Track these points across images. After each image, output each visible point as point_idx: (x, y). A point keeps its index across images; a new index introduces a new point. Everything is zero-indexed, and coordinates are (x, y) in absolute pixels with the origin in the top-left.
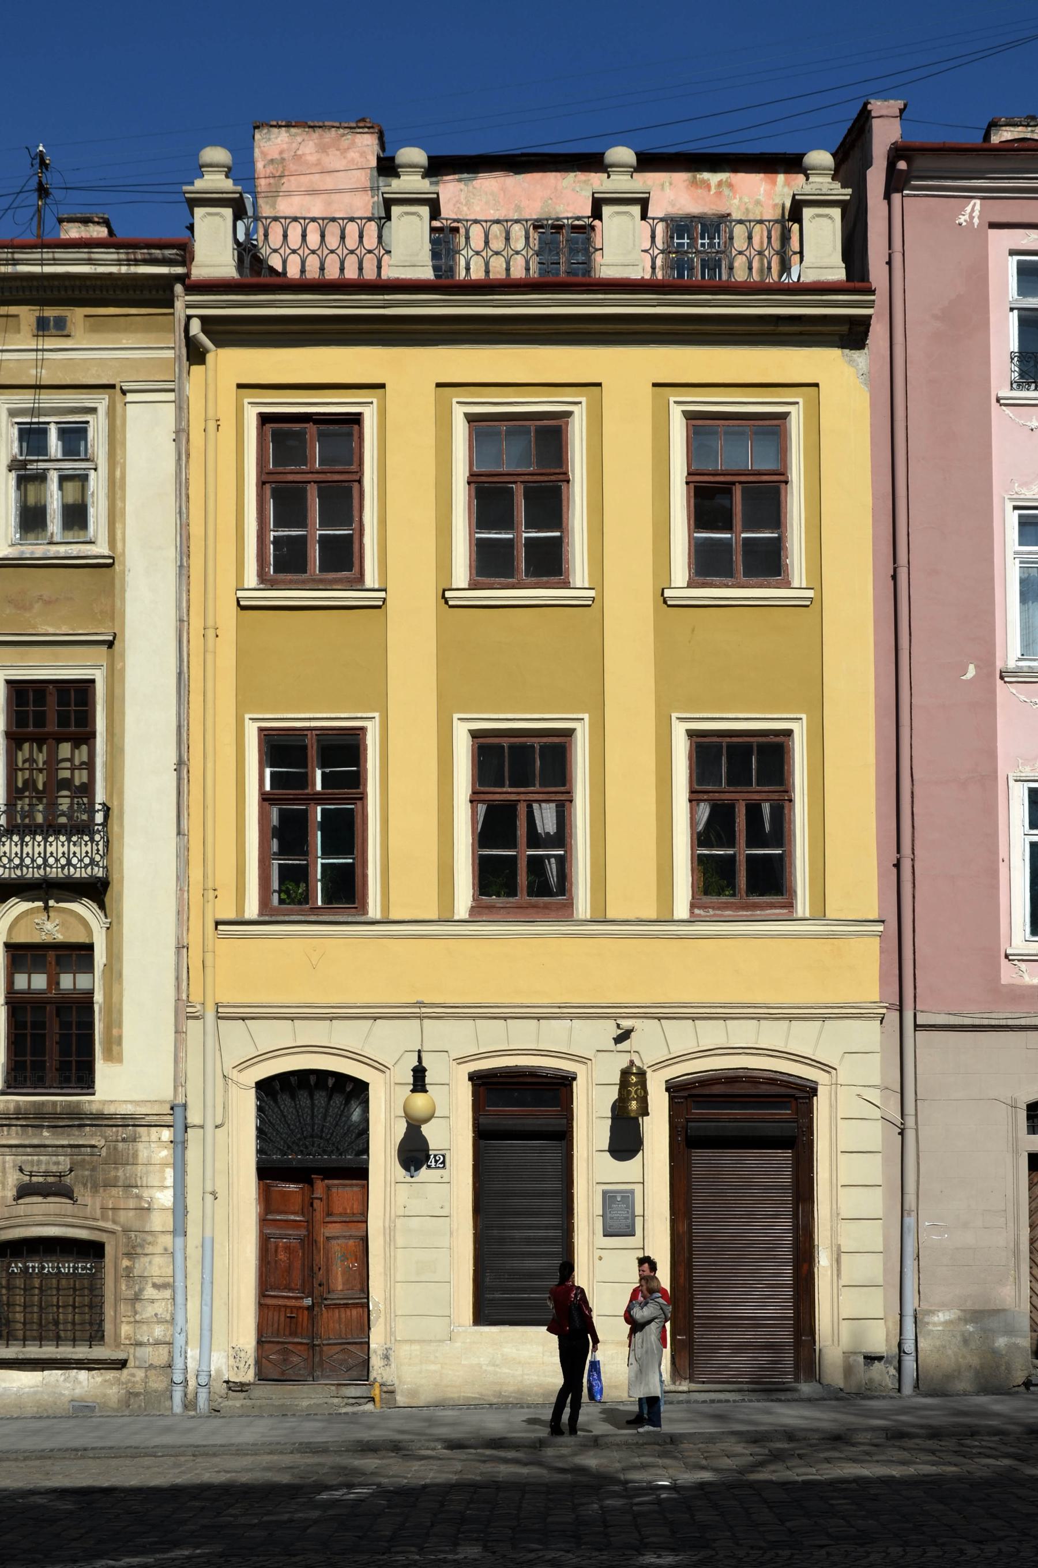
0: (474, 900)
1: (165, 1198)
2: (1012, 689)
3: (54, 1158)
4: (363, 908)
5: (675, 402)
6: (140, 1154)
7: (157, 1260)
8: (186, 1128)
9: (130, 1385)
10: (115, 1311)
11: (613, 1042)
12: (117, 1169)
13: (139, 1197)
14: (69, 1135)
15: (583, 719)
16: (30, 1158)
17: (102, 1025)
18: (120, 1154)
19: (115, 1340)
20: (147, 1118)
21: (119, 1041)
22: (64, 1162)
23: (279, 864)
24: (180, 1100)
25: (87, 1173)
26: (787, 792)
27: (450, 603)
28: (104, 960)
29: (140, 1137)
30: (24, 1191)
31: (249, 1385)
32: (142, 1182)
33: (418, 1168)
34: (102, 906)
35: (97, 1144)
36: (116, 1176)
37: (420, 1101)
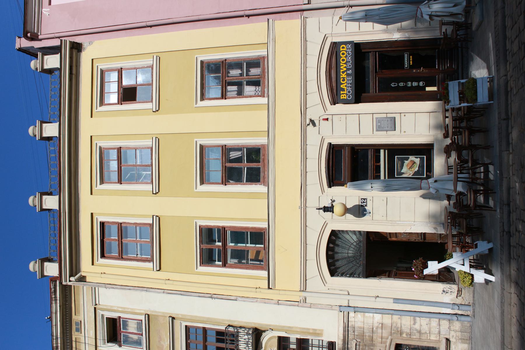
0: (261, 185)
1: (378, 317)
5: (96, 109)
6: (360, 326)
8: (349, 306)
9: (457, 338)
10: (425, 341)
11: (315, 127)
12: (365, 336)
13: (377, 328)
15: (196, 141)
18: (359, 334)
19: (437, 343)
20: (345, 321)
23: (250, 261)
24: (338, 308)
25: (367, 348)
26: (223, 61)
27: (157, 191)
28: (284, 333)
29: (353, 325)
31: (459, 288)
32: (371, 326)
33: (365, 210)
34: (264, 331)
35: (355, 343)
36: (369, 336)
37: (338, 209)
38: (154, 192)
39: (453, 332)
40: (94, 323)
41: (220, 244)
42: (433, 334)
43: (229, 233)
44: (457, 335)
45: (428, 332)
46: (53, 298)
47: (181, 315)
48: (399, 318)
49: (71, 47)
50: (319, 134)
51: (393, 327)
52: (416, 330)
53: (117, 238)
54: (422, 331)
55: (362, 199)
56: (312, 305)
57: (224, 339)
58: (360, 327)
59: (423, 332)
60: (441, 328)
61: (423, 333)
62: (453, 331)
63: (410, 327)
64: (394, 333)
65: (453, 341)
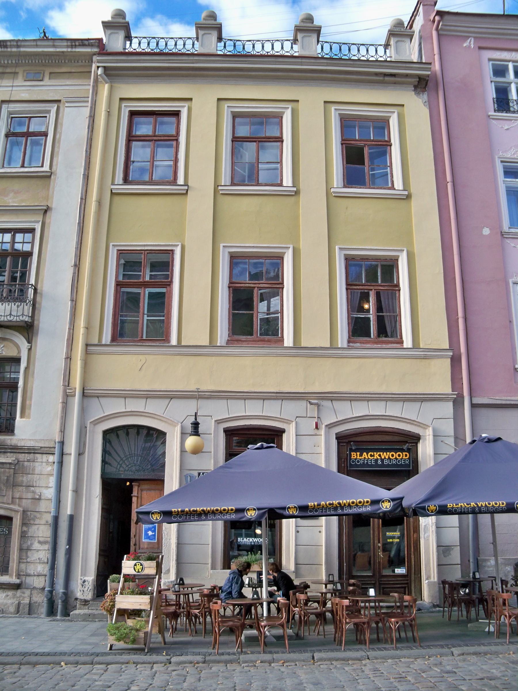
0: (229, 337)
2: (508, 241)
4: (167, 339)
12: (23, 476)
13: (34, 492)
31: (89, 601)
32: (36, 484)
36: (22, 480)
38: (220, 188)
39: (29, 593)
41: (147, 279)
43: (163, 290)
44: (25, 599)
45: (29, 560)
46: (75, 43)
47: (50, 222)
48: (47, 522)
49: (421, 77)
50: (297, 417)
51: (35, 513)
53: (157, 134)
54: (31, 552)
56: (65, 404)
57: (16, 282)
58: (34, 469)
60: (35, 578)
61: (27, 554)
62: (31, 594)
63: (35, 536)
65: (17, 592)
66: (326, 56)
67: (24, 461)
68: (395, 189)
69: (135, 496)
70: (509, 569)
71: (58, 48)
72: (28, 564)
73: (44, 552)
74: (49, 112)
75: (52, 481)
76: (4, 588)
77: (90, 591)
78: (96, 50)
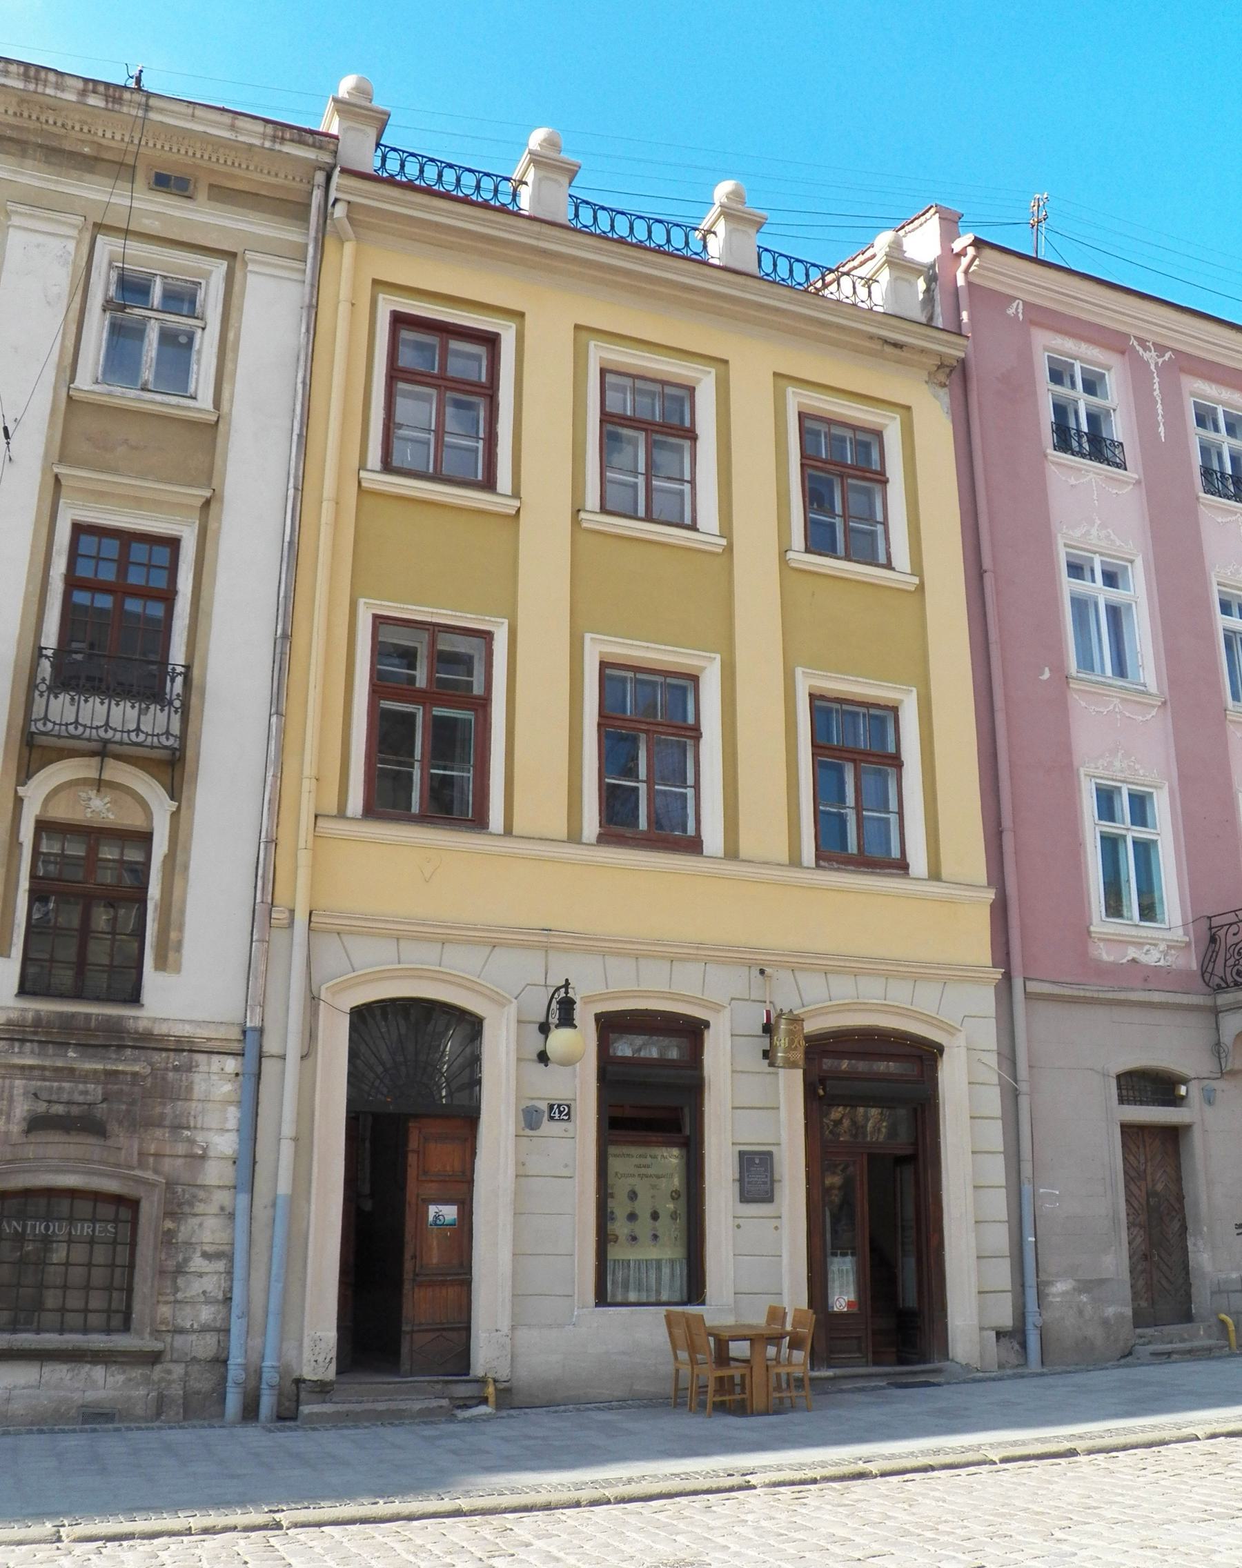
0: (600, 826)
3: (81, 1087)
6: (196, 1088)
7: (211, 1223)
12: (164, 1104)
13: (191, 1141)
14: (103, 1058)
16: (47, 1083)
17: (156, 926)
21: (179, 946)
22: (95, 1091)
24: (256, 1023)
25: (124, 1107)
29: (197, 1066)
30: (36, 1124)
32: (196, 1123)
35: (142, 1071)
36: (163, 1113)
39: (182, 1372)
40: (185, 239)
42: (174, 1311)
44: (173, 1386)
45: (180, 1296)
50: (733, 999)
51: (195, 1190)
52: (187, 1260)
55: (569, 1106)
59: (178, 1281)
60: (194, 1337)
61: (176, 1282)
62: (186, 1374)
63: (194, 1240)
64: (175, 1193)
65: (152, 1372)
66: (797, 287)
67: (167, 1069)
68: (893, 569)
69: (413, 1151)
70: (1085, 1300)
71: (242, 134)
72: (178, 1306)
73: (215, 1277)
74: (207, 275)
75: (232, 1116)
76: (123, 1363)
77: (330, 1362)
78: (326, 158)
